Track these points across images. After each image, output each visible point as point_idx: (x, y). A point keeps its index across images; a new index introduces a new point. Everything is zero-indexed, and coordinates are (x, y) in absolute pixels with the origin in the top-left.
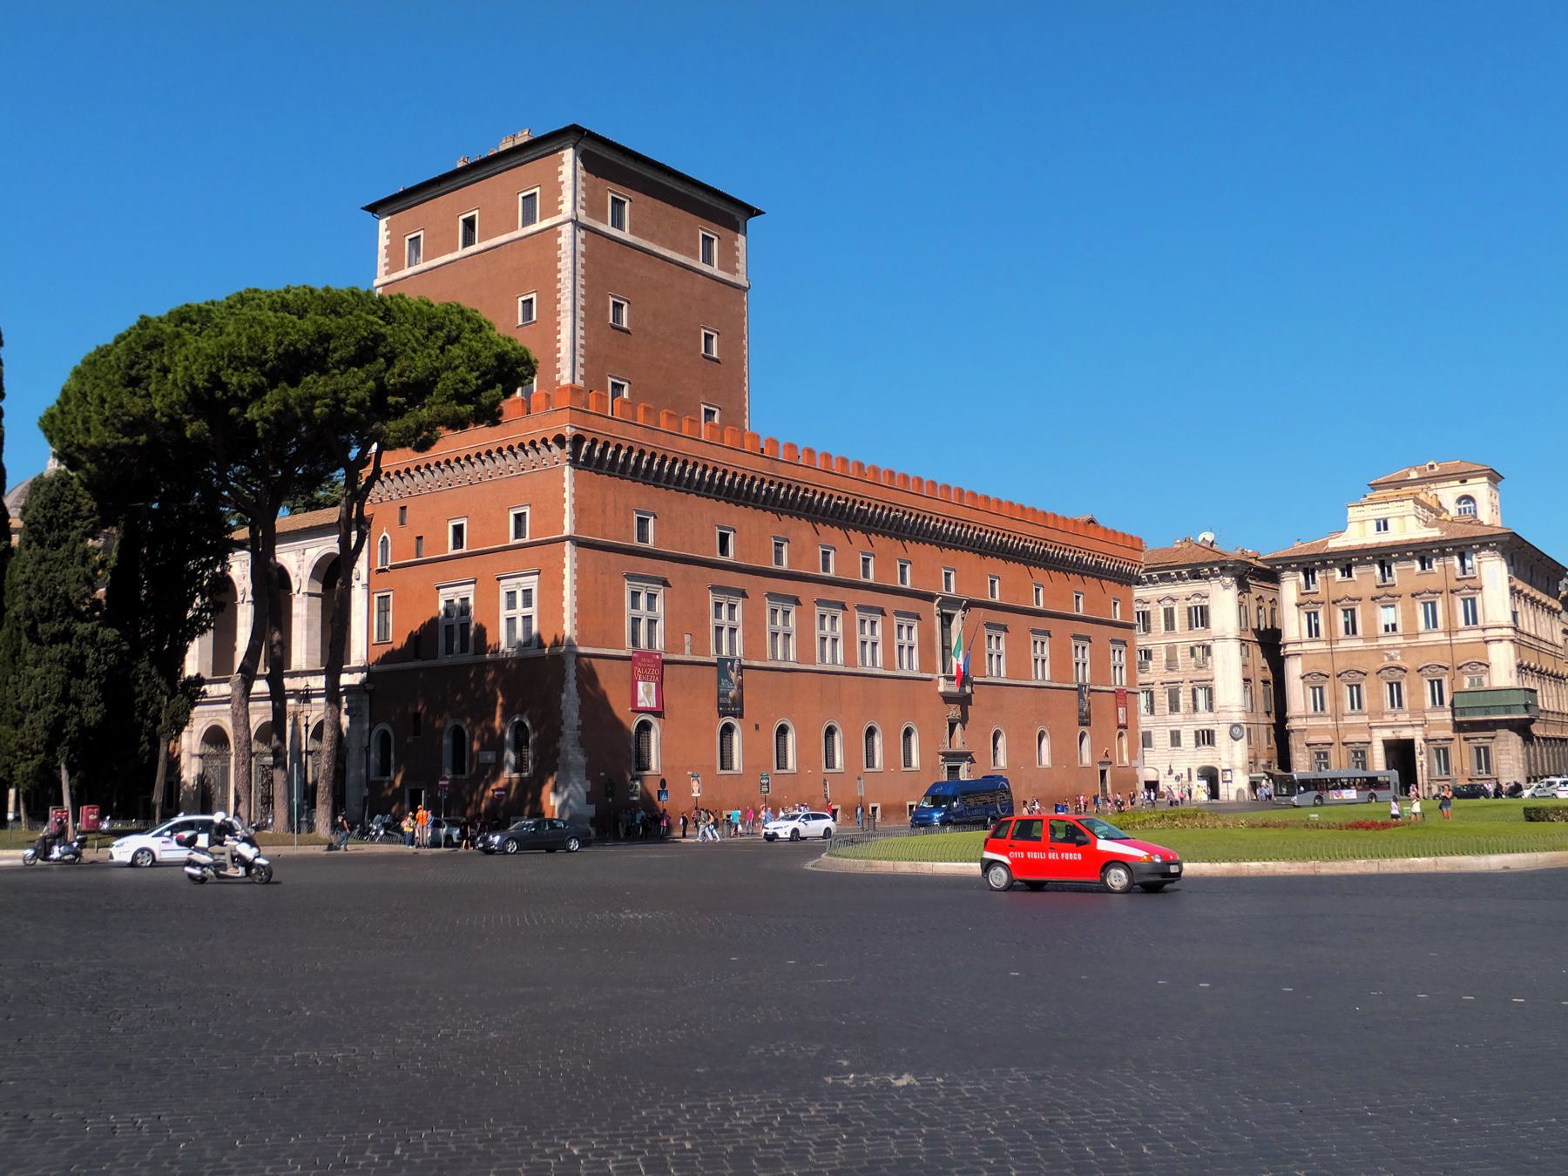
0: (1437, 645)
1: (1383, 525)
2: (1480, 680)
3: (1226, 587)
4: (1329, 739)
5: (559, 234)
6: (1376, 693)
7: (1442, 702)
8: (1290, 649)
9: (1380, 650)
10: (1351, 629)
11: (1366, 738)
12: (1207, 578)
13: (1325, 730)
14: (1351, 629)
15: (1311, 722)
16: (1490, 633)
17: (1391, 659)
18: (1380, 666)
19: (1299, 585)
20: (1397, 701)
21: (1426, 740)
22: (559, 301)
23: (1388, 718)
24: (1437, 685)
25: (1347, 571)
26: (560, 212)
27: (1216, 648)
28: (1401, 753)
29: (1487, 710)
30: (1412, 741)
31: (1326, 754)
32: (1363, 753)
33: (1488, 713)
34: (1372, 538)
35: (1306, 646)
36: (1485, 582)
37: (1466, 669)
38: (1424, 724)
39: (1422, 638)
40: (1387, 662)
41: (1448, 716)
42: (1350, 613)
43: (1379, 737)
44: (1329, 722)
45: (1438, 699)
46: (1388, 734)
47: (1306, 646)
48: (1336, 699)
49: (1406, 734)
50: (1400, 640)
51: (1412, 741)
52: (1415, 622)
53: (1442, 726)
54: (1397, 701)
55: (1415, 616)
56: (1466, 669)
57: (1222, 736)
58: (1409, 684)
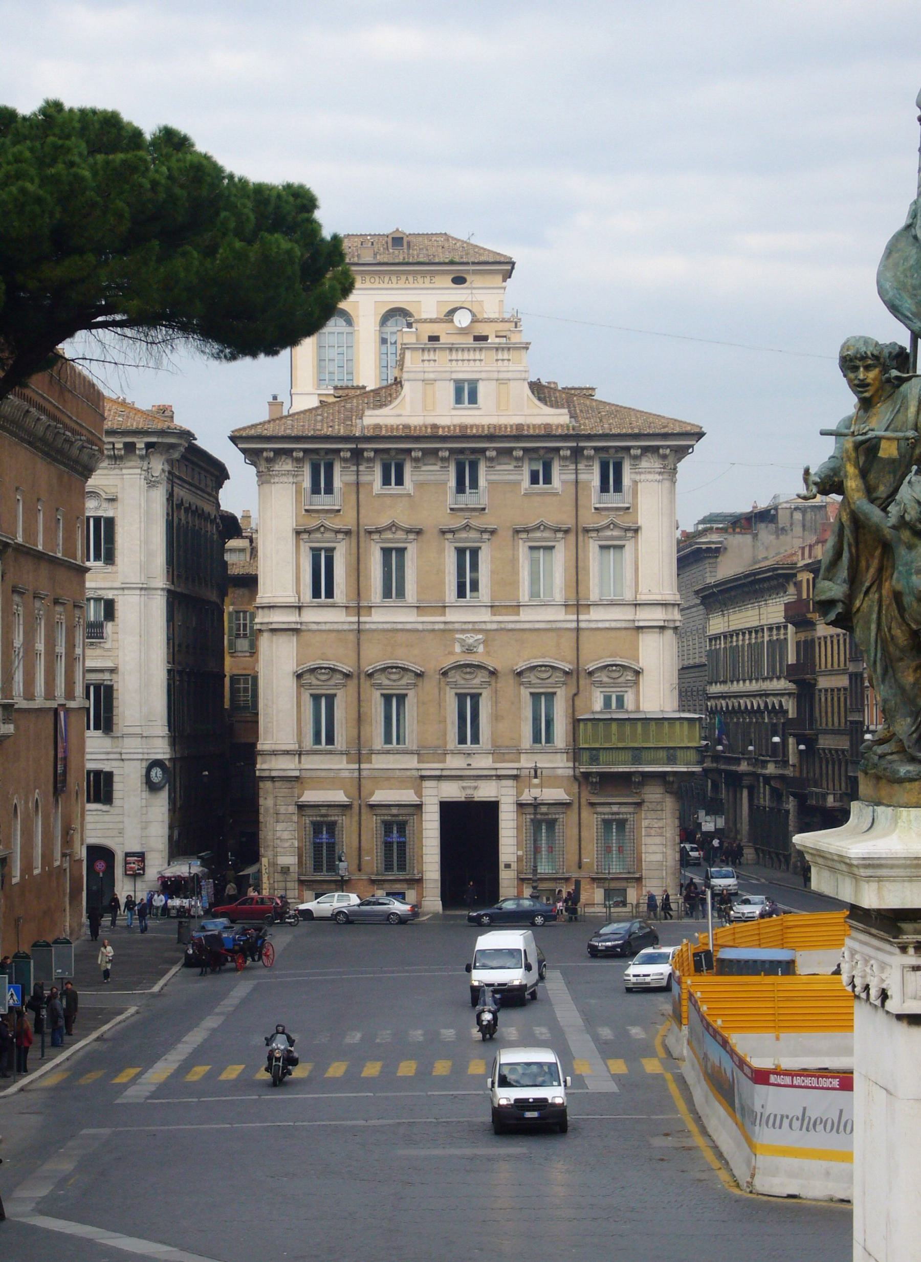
1: (466, 392)
3: (151, 484)
4: (339, 797)
9: (447, 632)
10: (393, 587)
11: (407, 796)
14: (393, 587)
15: (310, 763)
17: (469, 650)
18: (447, 662)
19: (298, 492)
20: (468, 728)
23: (455, 763)
25: (393, 473)
27: (128, 608)
28: (470, 828)
29: (637, 754)
30: (491, 809)
31: (332, 827)
32: (402, 827)
33: (637, 760)
34: (447, 415)
35: (310, 616)
36: (641, 522)
37: (598, 677)
38: (518, 772)
39: (526, 616)
40: (458, 655)
41: (561, 764)
42: (393, 557)
43: (434, 796)
44: (340, 764)
46: (453, 792)
47: (310, 616)
48: (360, 719)
49: (485, 792)
50: (485, 616)
51: (491, 809)
52: (514, 584)
54: (468, 728)
55: (515, 571)
56: (603, 677)
58: (496, 703)
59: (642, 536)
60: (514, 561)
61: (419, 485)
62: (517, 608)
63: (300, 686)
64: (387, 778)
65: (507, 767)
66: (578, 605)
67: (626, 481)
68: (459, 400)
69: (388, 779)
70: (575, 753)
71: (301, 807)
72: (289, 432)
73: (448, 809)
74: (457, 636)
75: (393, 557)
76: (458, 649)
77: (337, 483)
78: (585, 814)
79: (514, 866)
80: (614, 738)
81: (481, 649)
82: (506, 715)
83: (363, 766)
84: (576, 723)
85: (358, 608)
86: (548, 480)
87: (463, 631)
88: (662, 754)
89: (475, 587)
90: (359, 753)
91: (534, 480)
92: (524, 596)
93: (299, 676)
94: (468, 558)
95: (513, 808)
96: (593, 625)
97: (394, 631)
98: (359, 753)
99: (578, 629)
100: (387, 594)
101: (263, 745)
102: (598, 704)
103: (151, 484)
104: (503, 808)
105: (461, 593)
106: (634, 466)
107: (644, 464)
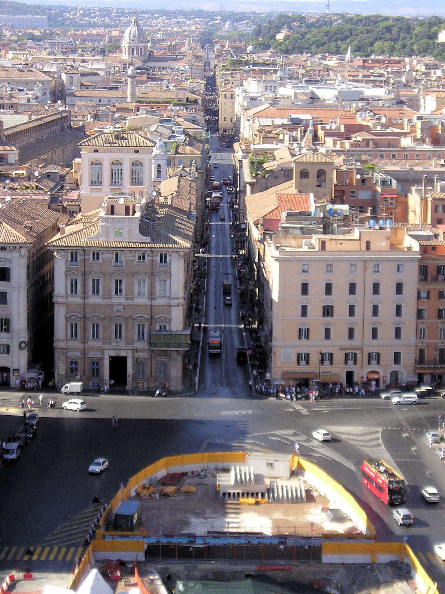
2: (165, 327)
3: (21, 257)
4: (78, 354)
6: (107, 330)
7: (143, 337)
8: (60, 300)
10: (96, 291)
11: (98, 355)
12: (10, 251)
13: (77, 349)
14: (96, 291)
16: (173, 302)
17: (118, 311)
19: (67, 261)
20: (118, 334)
21: (133, 358)
28: (118, 364)
30: (125, 359)
31: (76, 363)
32: (97, 363)
42: (95, 283)
45: (141, 336)
46: (113, 353)
49: (123, 354)
51: (125, 359)
52: (133, 291)
53: (143, 351)
54: (118, 334)
57: (14, 348)
58: (126, 326)
59: (173, 277)
60: (133, 284)
61: (103, 260)
62: (133, 299)
63: (66, 321)
64: (93, 349)
66: (152, 297)
67: (168, 260)
69: (93, 349)
70: (150, 343)
72: (63, 244)
74: (115, 306)
75: (95, 283)
76: (115, 310)
77: (79, 259)
78: (153, 361)
79: (131, 376)
80: (162, 340)
81: (122, 310)
82: (130, 331)
83: (86, 345)
85: (85, 296)
86: (144, 259)
87: (117, 305)
88: (176, 345)
89: (121, 291)
90: (84, 341)
91: (140, 259)
94: (118, 283)
95: (131, 359)
96: (157, 304)
97: (95, 305)
98: (84, 341)
99: (152, 305)
100: (94, 293)
101: (55, 338)
102: (158, 328)
103: (21, 257)
105: (116, 293)
106: (171, 256)
107: (173, 255)
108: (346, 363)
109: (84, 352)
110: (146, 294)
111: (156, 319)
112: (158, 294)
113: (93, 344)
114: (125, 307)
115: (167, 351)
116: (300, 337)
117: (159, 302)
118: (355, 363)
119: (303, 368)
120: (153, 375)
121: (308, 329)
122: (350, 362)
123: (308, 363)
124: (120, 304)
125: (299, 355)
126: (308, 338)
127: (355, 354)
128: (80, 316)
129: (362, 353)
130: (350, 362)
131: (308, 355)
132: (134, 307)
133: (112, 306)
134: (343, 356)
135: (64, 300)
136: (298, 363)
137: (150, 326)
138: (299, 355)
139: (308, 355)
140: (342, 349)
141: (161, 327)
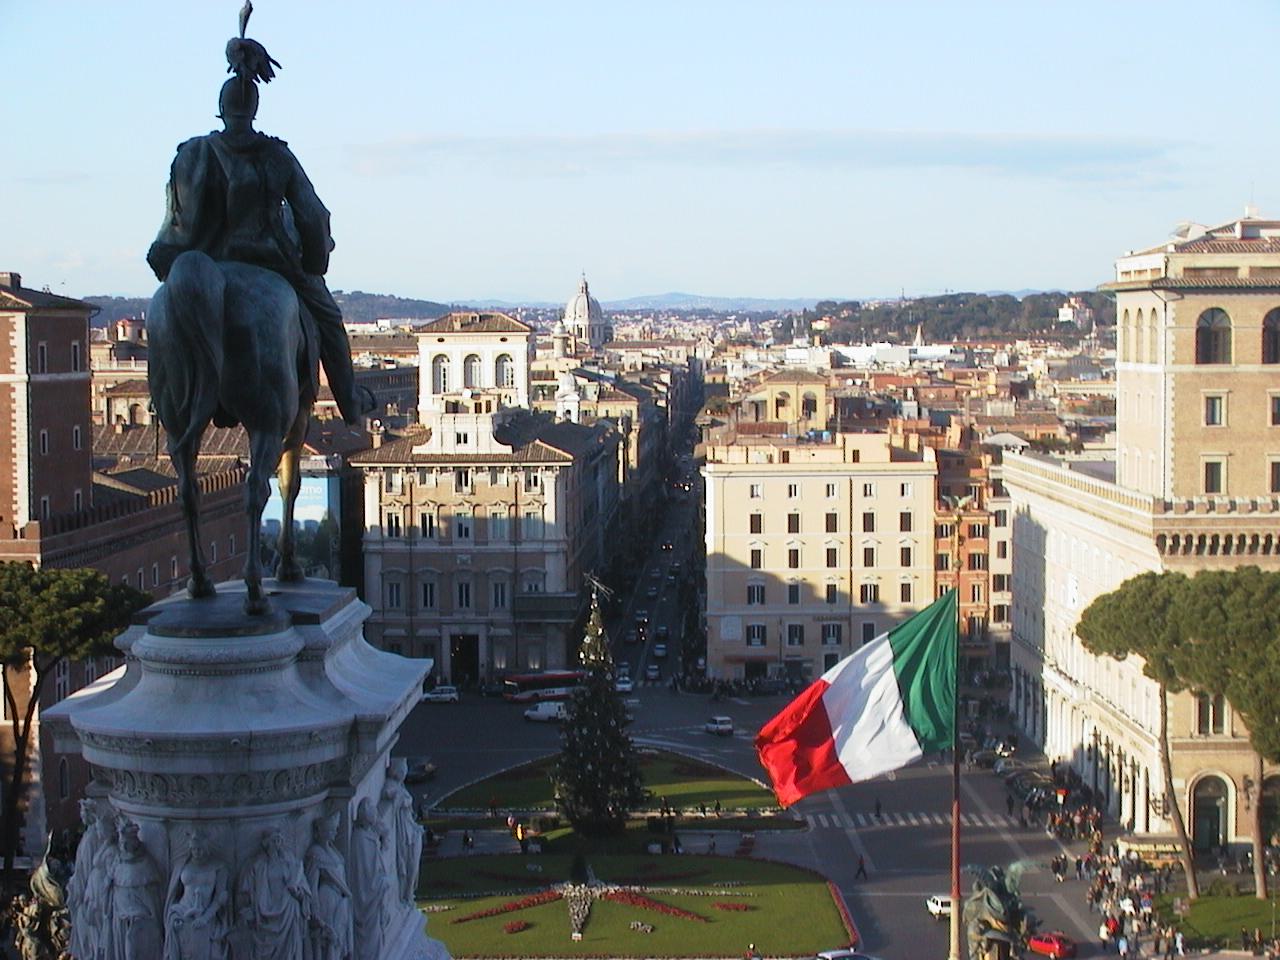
0: (504, 553)
2: (536, 587)
4: (402, 632)
5: (14, 390)
8: (372, 547)
11: (434, 632)
16: (549, 547)
17: (464, 562)
20: (464, 599)
21: (491, 639)
22: (15, 446)
23: (457, 617)
24: (499, 588)
26: (13, 372)
30: (475, 639)
34: (452, 448)
41: (507, 617)
43: (447, 632)
44: (405, 618)
45: (499, 602)
46: (456, 630)
47: (388, 546)
48: (412, 596)
49: (472, 630)
50: (472, 547)
51: (475, 639)
54: (464, 599)
62: (486, 543)
65: (483, 618)
68: (459, 441)
70: (514, 613)
71: (384, 637)
73: (453, 638)
74: (460, 556)
76: (458, 562)
81: (470, 562)
83: (414, 618)
84: (514, 601)
92: (490, 537)
93: (382, 575)
97: (427, 555)
99: (516, 554)
102: (526, 589)
104: (480, 638)
105: (460, 535)
108: (824, 641)
109: (411, 627)
110: (507, 537)
111: (522, 574)
112: (524, 536)
113: (426, 615)
114: (474, 556)
115: (539, 624)
116: (750, 601)
117: (526, 547)
118: (839, 641)
119: (756, 650)
120: (519, 663)
121: (763, 588)
122: (832, 640)
123: (764, 642)
124: (466, 552)
125: (748, 628)
126: (763, 602)
127: (839, 627)
128: (404, 571)
129: (850, 625)
130: (832, 640)
131: (764, 628)
132: (491, 556)
133: (453, 555)
134: (820, 629)
135: (378, 547)
136: (749, 642)
137: (513, 588)
138: (748, 628)
139: (764, 628)
140: (817, 618)
141: (530, 587)
